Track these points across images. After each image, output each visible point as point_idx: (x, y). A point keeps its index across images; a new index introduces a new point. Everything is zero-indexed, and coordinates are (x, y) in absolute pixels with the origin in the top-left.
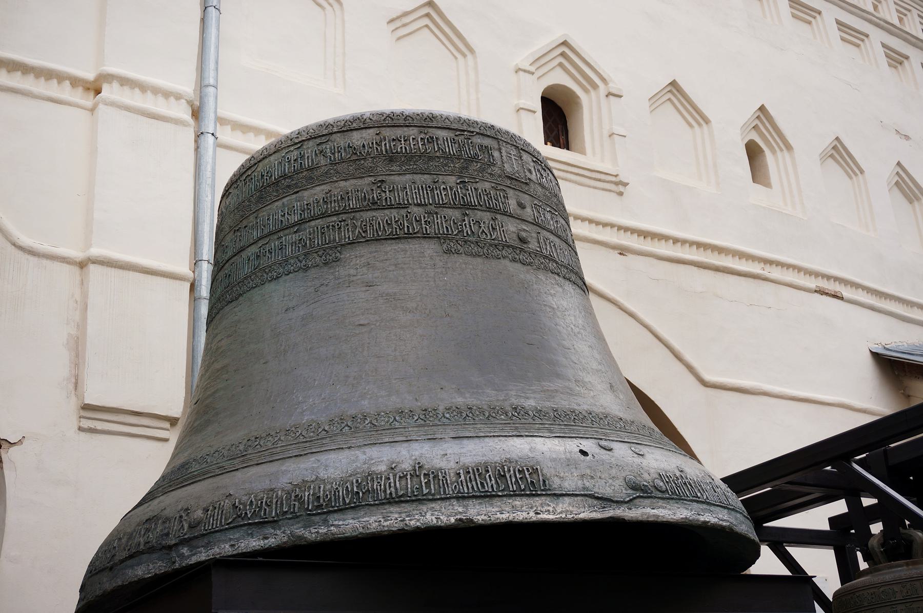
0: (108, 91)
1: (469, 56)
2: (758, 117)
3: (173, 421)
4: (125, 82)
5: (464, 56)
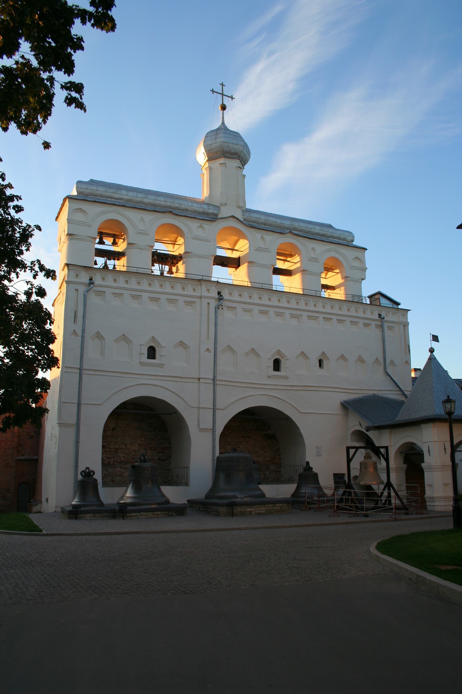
0: (201, 381)
1: (259, 357)
2: (323, 354)
3: (211, 429)
5: (259, 357)
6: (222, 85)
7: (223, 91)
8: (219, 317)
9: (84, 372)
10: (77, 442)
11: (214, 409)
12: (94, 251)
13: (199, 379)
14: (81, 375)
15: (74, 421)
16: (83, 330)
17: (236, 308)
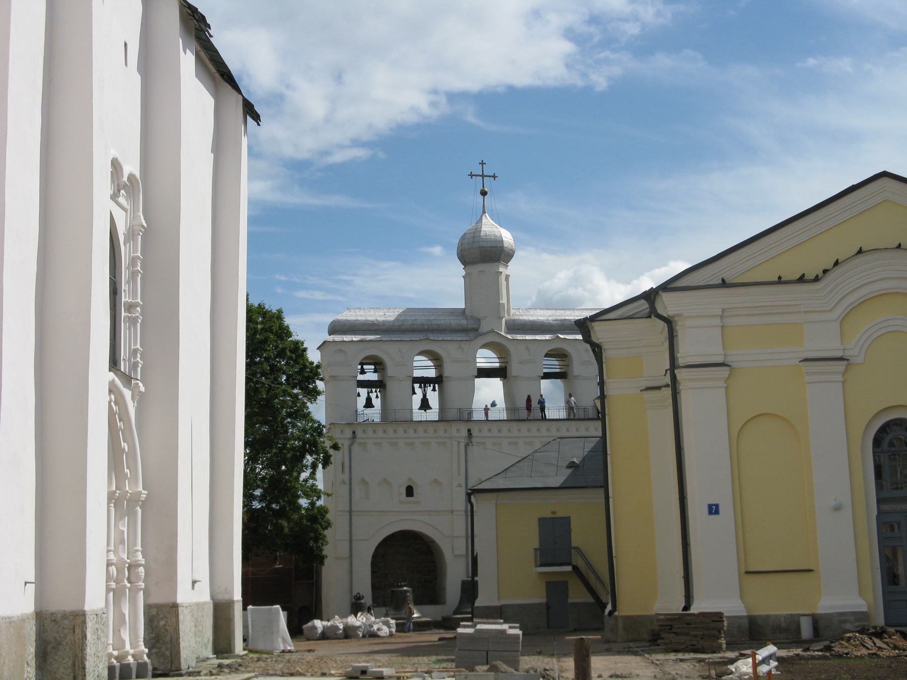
0: (455, 513)
4: (456, 511)
6: (482, 164)
7: (483, 171)
8: (469, 454)
9: (353, 514)
10: (351, 572)
11: (466, 537)
12: (356, 383)
13: (453, 512)
14: (351, 516)
15: (348, 555)
16: (350, 479)
17: (485, 443)
